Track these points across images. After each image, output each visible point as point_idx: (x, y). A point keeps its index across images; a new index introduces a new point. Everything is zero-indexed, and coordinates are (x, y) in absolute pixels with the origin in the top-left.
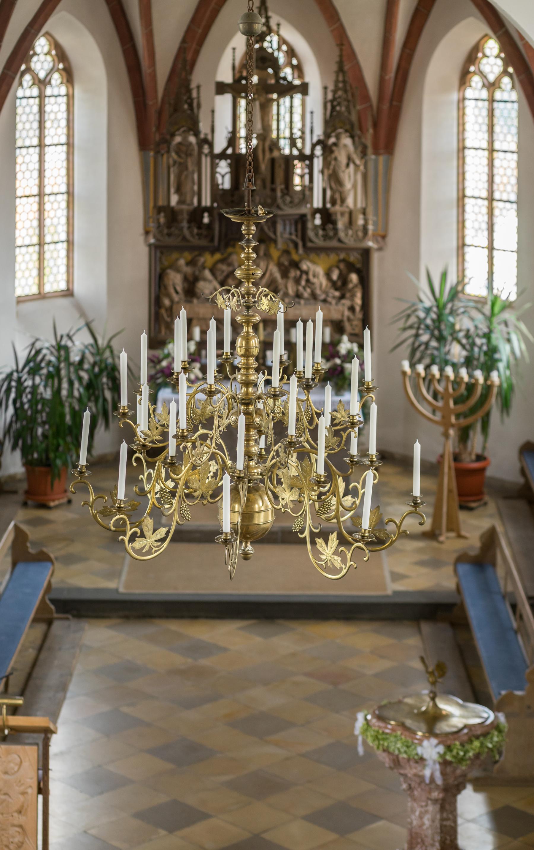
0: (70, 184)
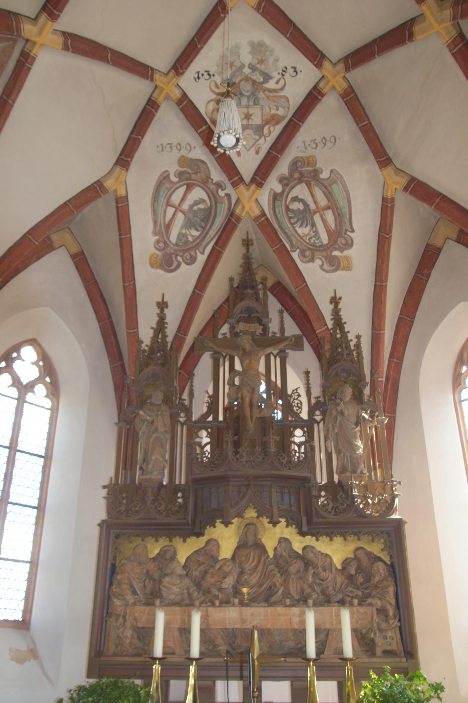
0: (42, 499)
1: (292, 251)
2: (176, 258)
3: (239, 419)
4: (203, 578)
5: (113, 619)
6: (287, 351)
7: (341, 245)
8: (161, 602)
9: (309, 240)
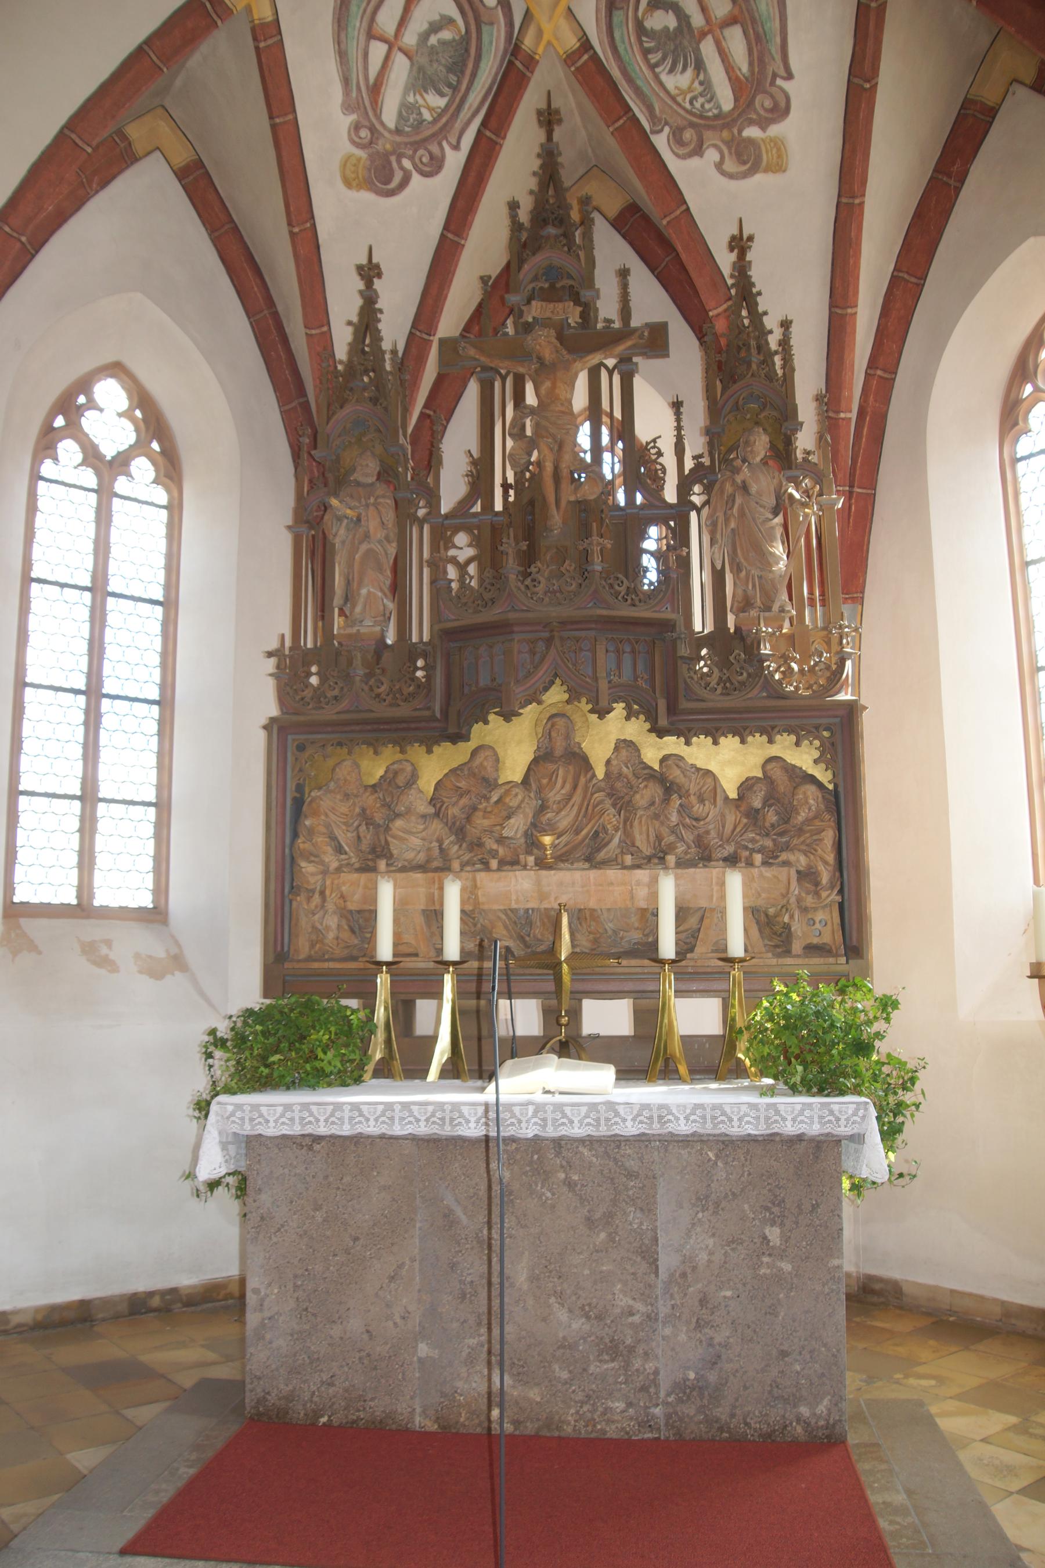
1: (654, 132)
2: (399, 162)
3: (533, 506)
4: (468, 819)
5: (301, 898)
6: (635, 359)
7: (762, 112)
8: (388, 865)
9: (691, 103)
